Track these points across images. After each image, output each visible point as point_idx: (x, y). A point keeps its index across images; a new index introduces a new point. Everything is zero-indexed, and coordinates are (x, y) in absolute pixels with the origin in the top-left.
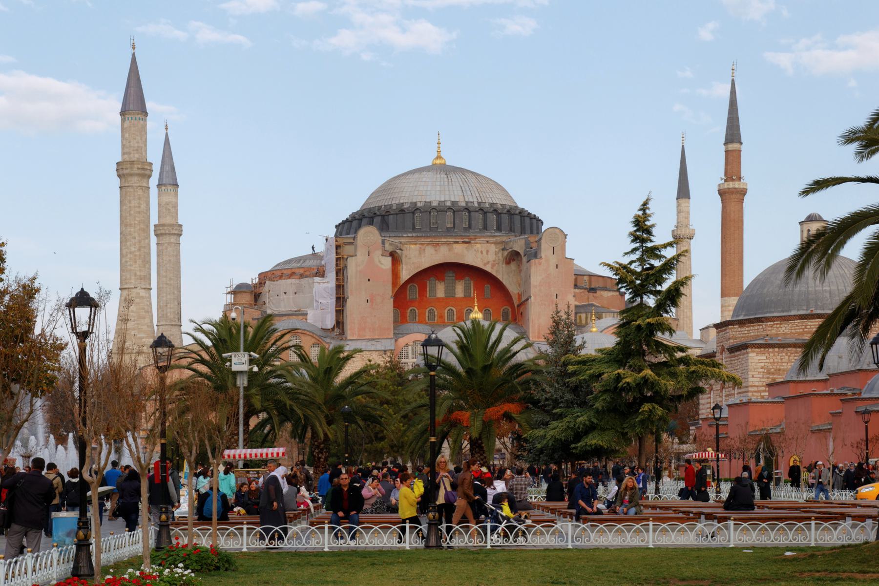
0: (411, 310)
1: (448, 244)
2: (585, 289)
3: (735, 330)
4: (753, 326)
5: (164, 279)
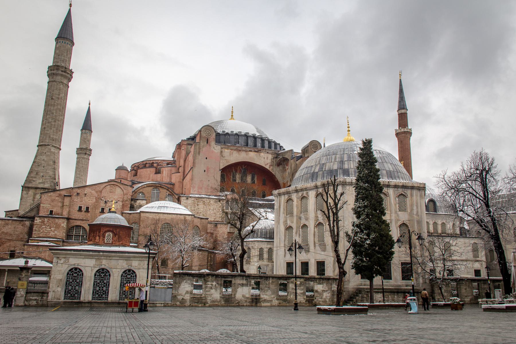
1: (246, 151)
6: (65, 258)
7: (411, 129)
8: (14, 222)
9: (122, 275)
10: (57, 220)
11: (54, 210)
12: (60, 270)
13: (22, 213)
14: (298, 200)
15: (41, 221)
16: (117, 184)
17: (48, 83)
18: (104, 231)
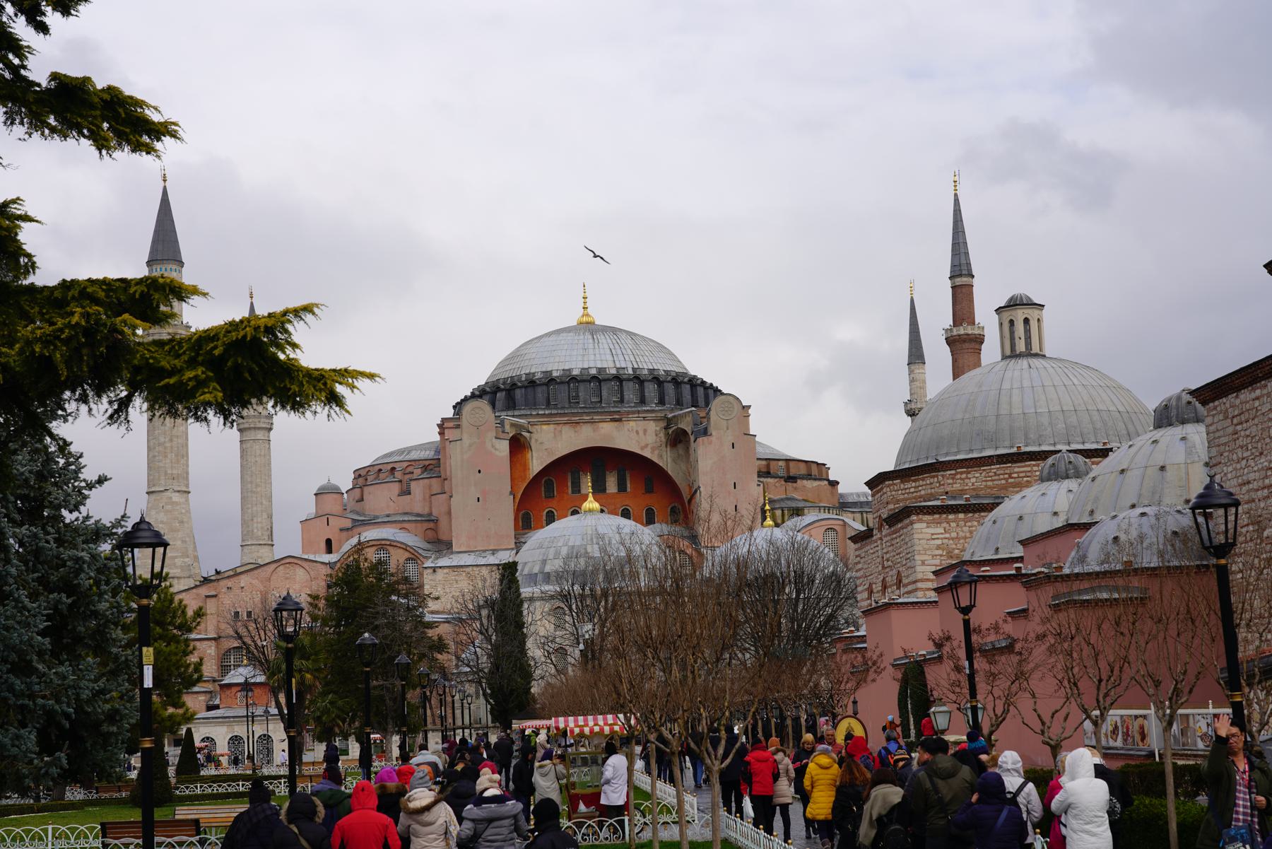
0: (548, 512)
2: (781, 478)
3: (896, 488)
4: (923, 479)
16: (296, 561)
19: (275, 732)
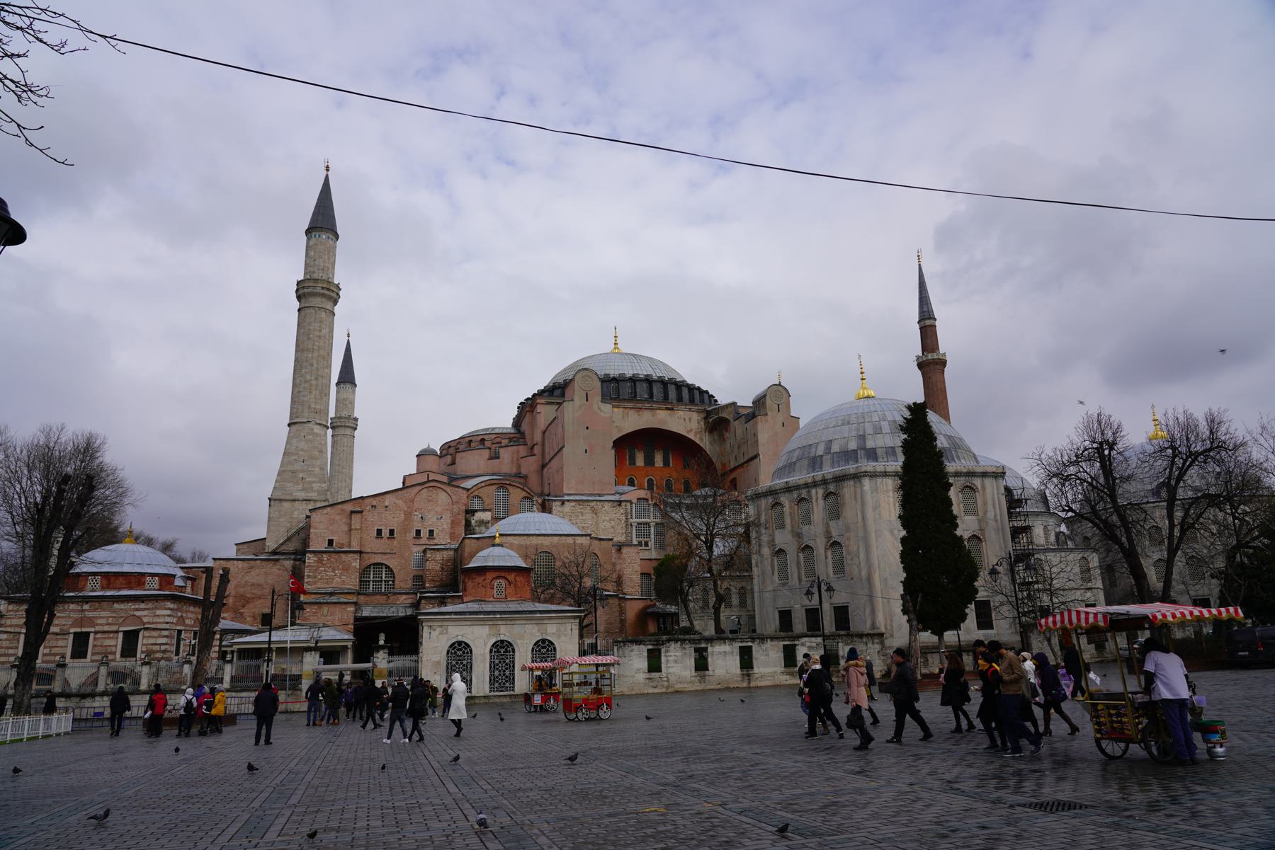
5: (337, 468)
6: (441, 626)
7: (944, 354)
8: (264, 563)
9: (533, 649)
10: (343, 556)
11: (334, 538)
12: (436, 647)
13: (271, 545)
14: (793, 504)
15: (316, 559)
16: (439, 485)
17: (299, 310)
18: (490, 578)
19: (559, 637)
